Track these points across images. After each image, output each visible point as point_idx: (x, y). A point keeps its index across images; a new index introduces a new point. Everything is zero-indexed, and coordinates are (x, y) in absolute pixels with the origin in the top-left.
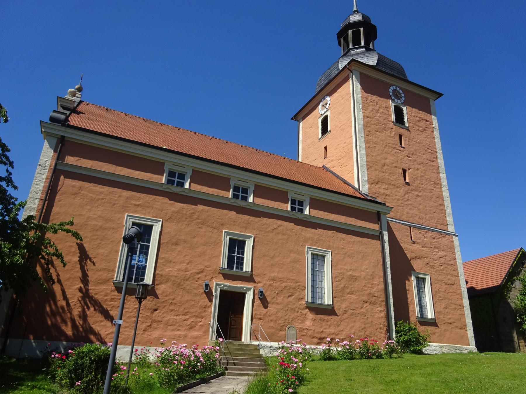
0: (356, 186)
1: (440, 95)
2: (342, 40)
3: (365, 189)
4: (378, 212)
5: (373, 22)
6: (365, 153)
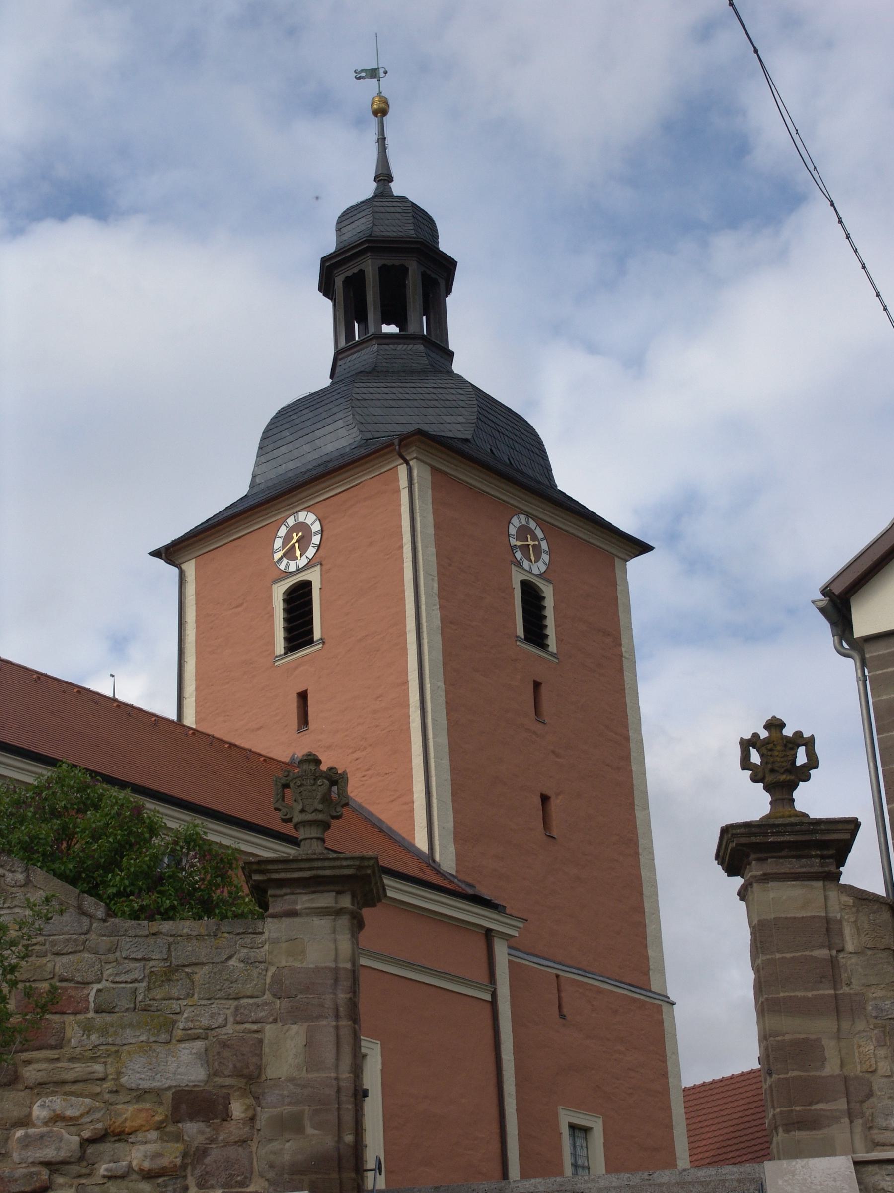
0: (421, 843)
1: (641, 548)
2: (339, 282)
3: (446, 858)
4: (489, 934)
5: (446, 245)
6: (447, 741)
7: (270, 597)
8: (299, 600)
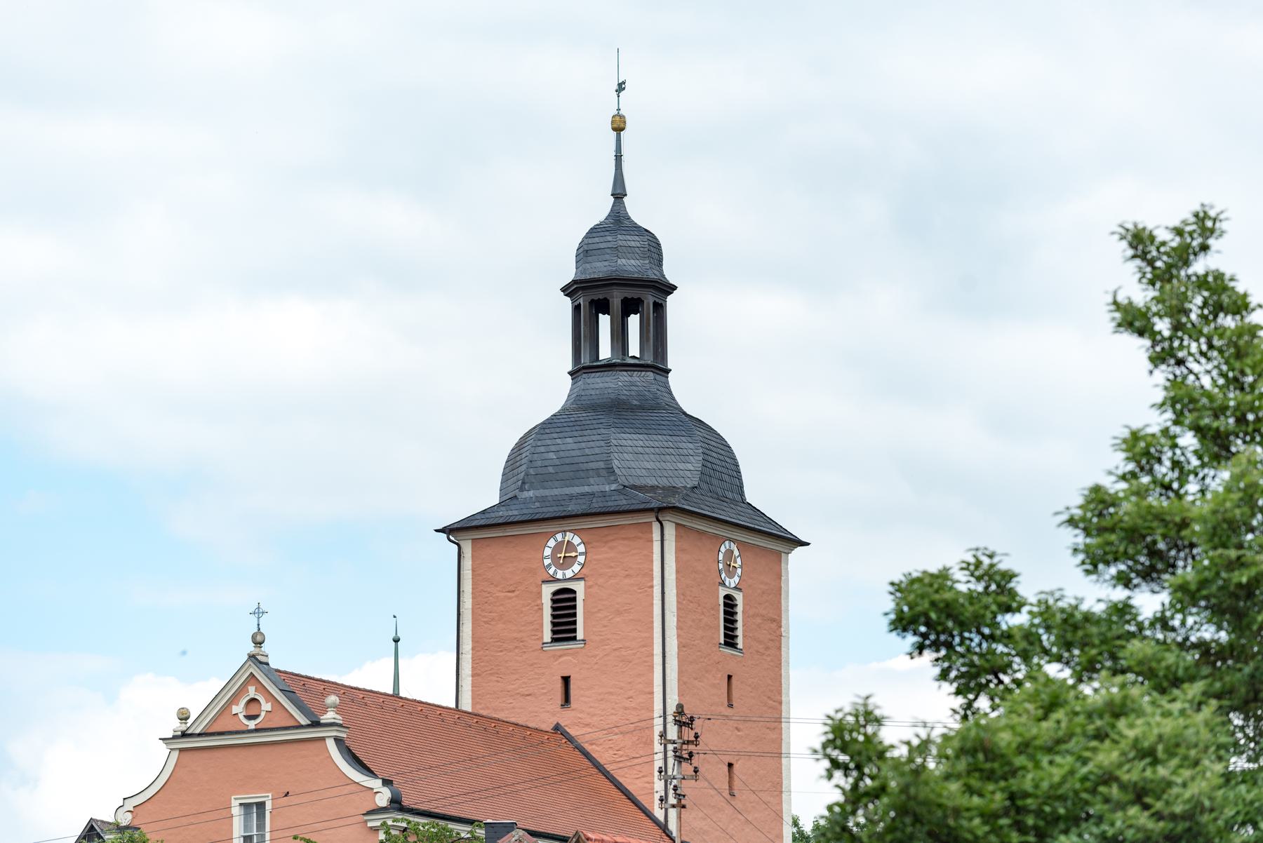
7: (540, 594)
8: (564, 603)
